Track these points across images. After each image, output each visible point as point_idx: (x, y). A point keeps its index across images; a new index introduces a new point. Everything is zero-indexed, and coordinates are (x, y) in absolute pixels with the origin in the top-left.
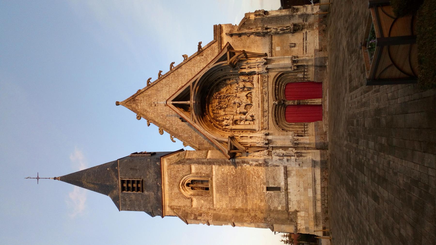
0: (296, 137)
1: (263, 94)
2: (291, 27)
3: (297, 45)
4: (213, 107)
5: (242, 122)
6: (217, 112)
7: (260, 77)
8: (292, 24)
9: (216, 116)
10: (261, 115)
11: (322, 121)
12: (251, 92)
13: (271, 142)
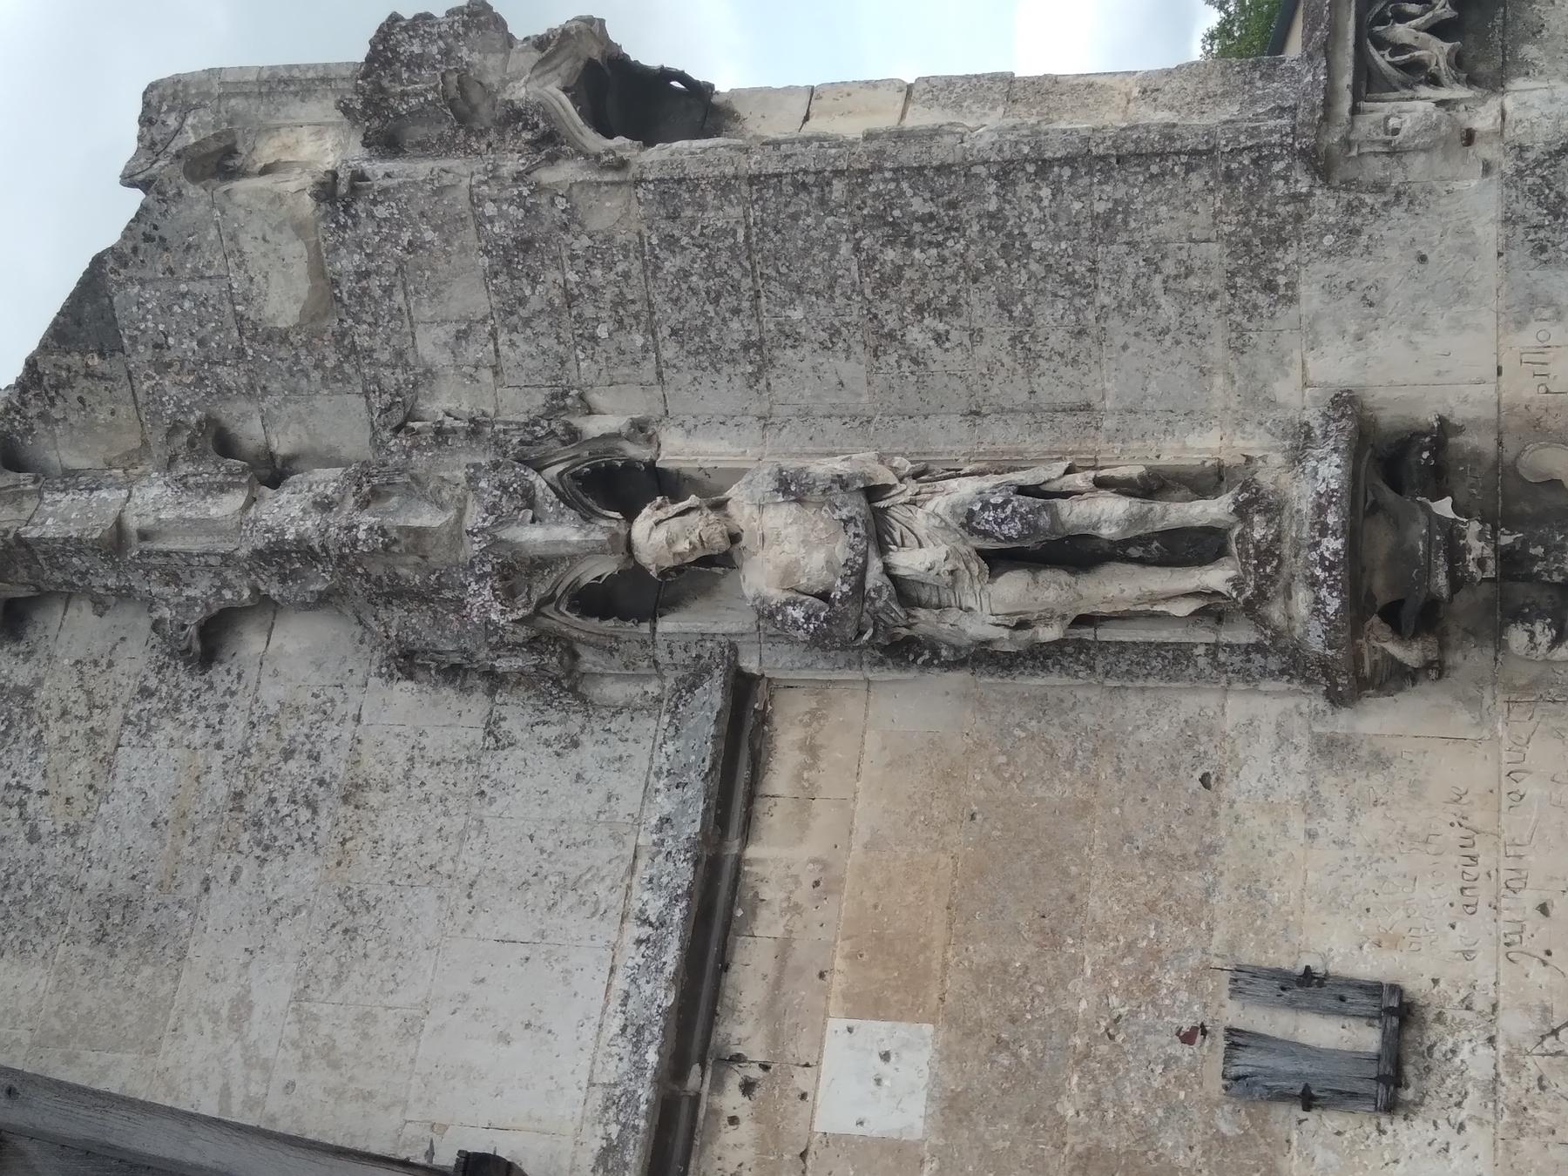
2: (1272, 474)
3: (1476, 1060)
8: (1313, 417)
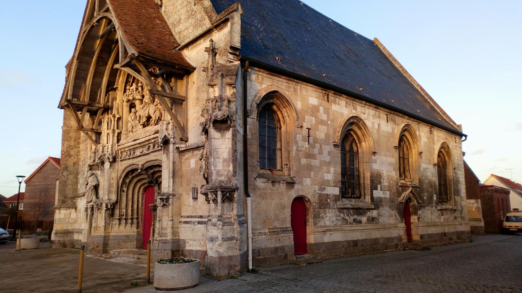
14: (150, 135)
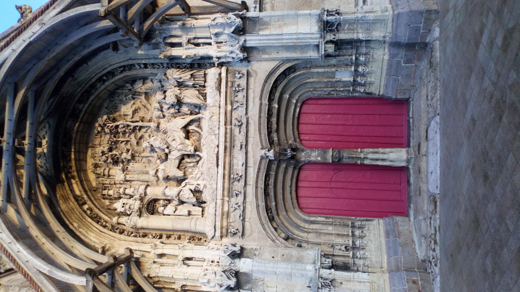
0: (328, 271)
1: (231, 124)
4: (95, 157)
5: (171, 204)
6: (106, 172)
7: (224, 75)
9: (103, 184)
10: (223, 190)
11: (407, 219)
12: (199, 118)
13: (248, 282)
14: (220, 107)
